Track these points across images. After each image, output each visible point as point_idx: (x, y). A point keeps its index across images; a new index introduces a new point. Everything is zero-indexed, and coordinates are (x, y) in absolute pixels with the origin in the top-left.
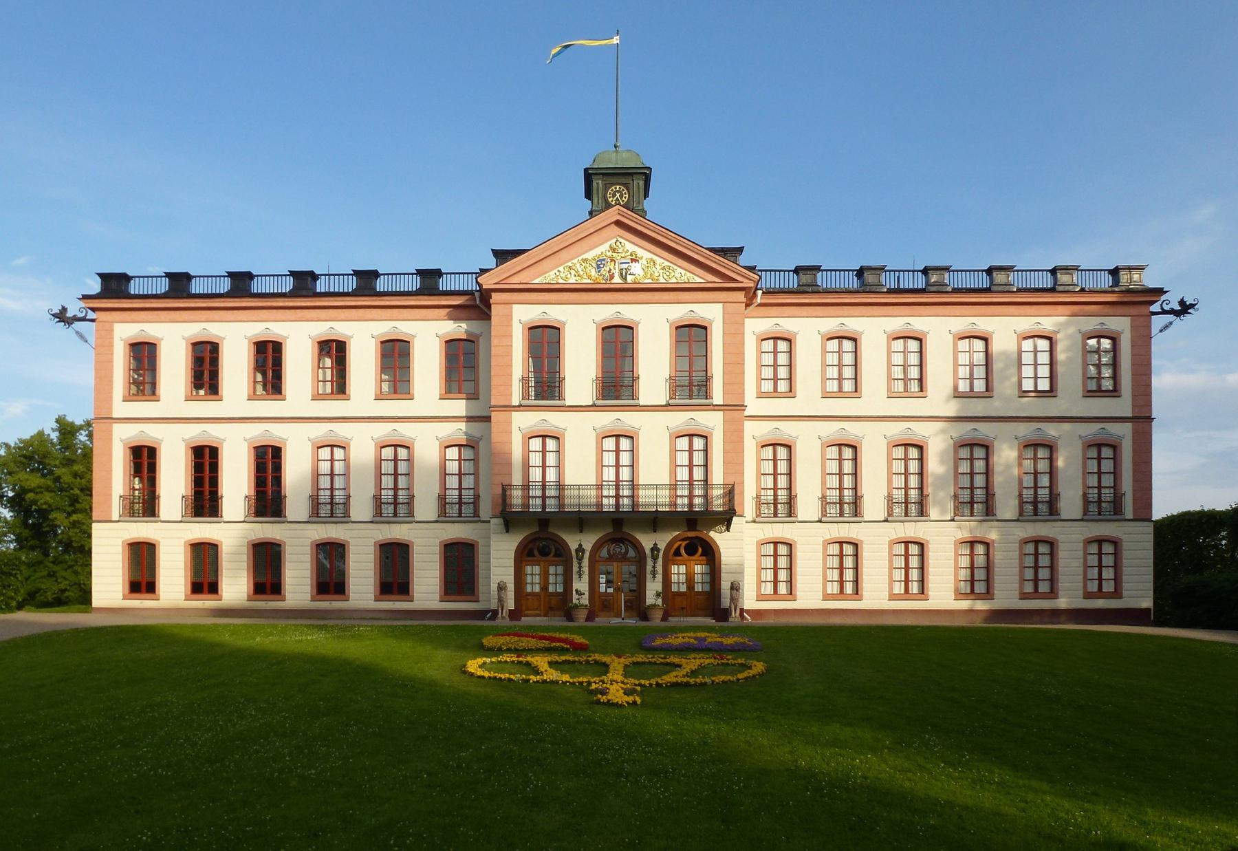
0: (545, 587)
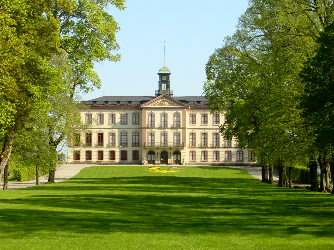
0: (151, 159)
